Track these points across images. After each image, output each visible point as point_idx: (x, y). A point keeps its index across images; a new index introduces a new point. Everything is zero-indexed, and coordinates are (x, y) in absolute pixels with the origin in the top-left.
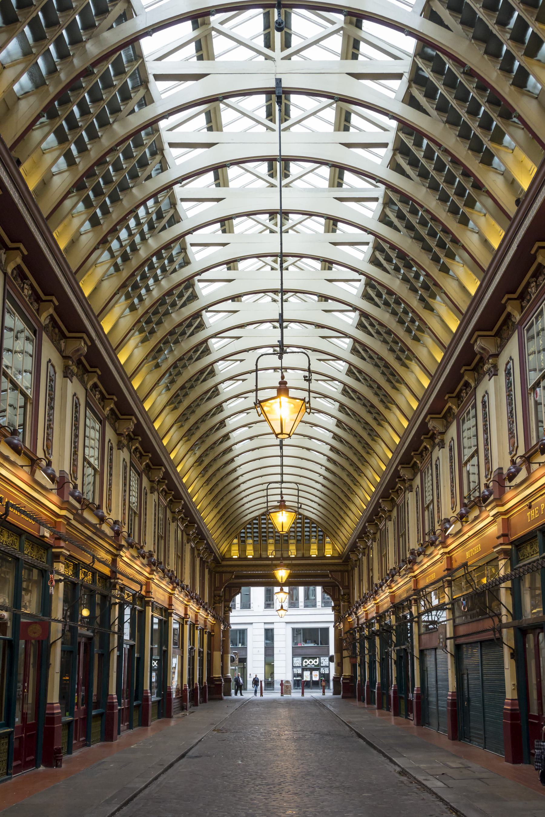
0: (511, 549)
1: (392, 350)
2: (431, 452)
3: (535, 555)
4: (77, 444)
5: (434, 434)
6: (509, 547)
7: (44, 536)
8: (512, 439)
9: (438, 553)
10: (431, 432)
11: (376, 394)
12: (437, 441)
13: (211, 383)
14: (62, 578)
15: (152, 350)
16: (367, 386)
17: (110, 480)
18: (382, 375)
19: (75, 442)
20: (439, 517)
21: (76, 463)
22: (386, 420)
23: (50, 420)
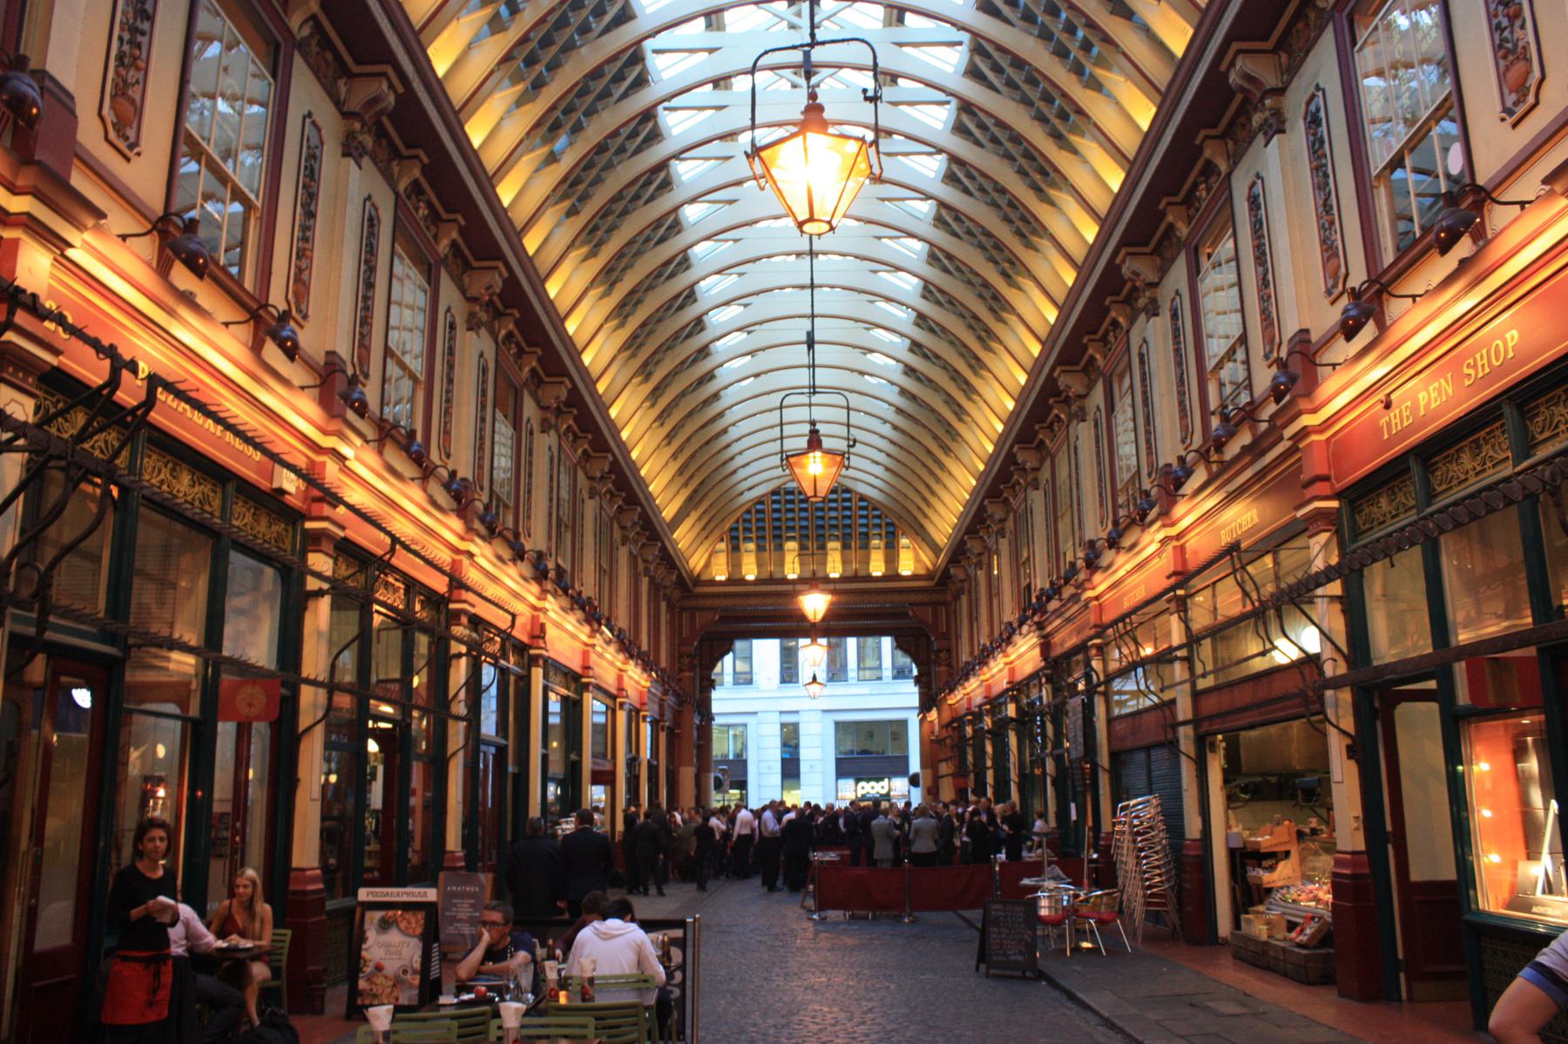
0: (1338, 509)
1: (1041, 119)
2: (1128, 331)
3: (1402, 517)
4: (370, 303)
5: (1134, 289)
6: (1334, 504)
7: (282, 492)
8: (1333, 261)
9: (1151, 539)
10: (1128, 286)
11: (1007, 220)
12: (1142, 302)
13: (665, 203)
14: (326, 586)
15: (538, 125)
16: (987, 203)
17: (448, 391)
18: (1018, 176)
19: (366, 298)
20: (1150, 464)
21: (366, 342)
22: (1029, 271)
23: (305, 239)
